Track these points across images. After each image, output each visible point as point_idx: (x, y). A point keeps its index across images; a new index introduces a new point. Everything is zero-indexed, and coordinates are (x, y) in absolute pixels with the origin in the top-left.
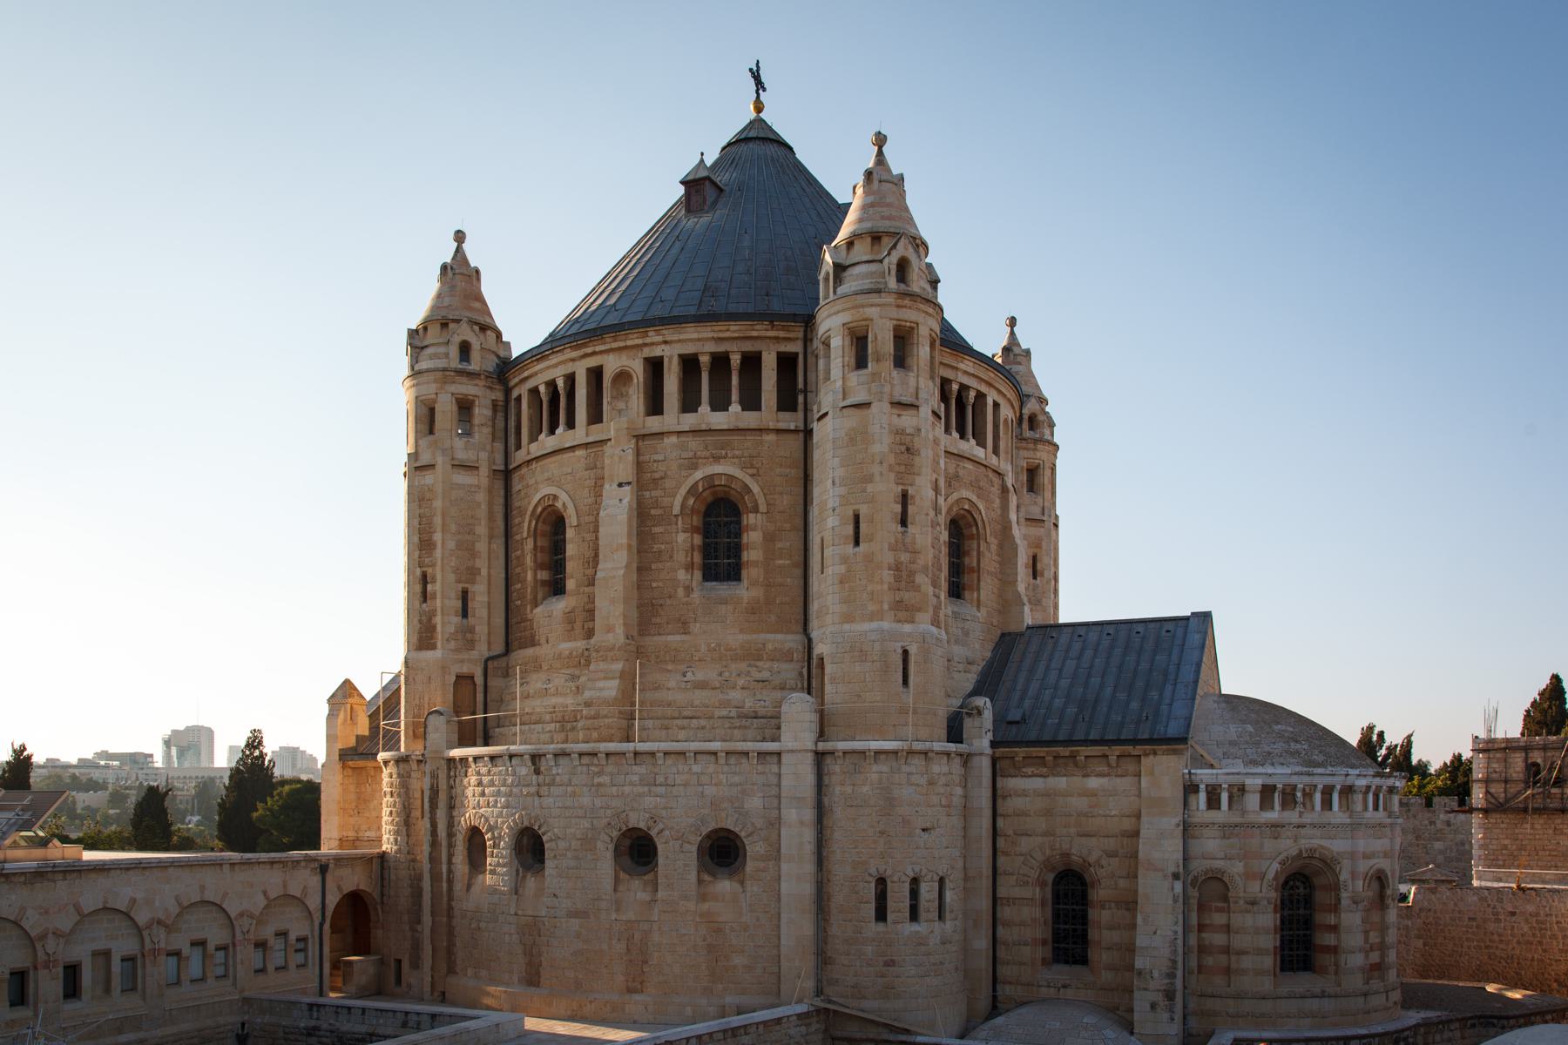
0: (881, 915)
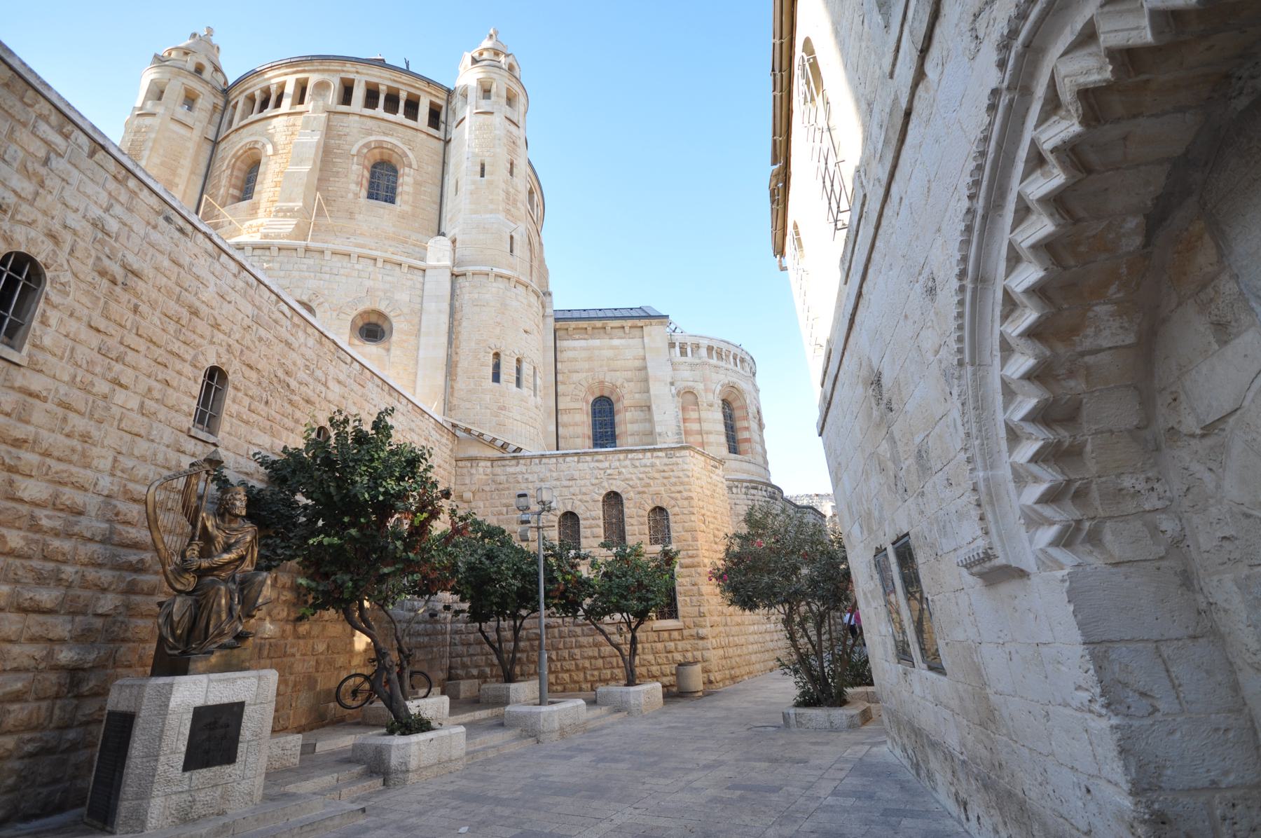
0: (496, 377)
